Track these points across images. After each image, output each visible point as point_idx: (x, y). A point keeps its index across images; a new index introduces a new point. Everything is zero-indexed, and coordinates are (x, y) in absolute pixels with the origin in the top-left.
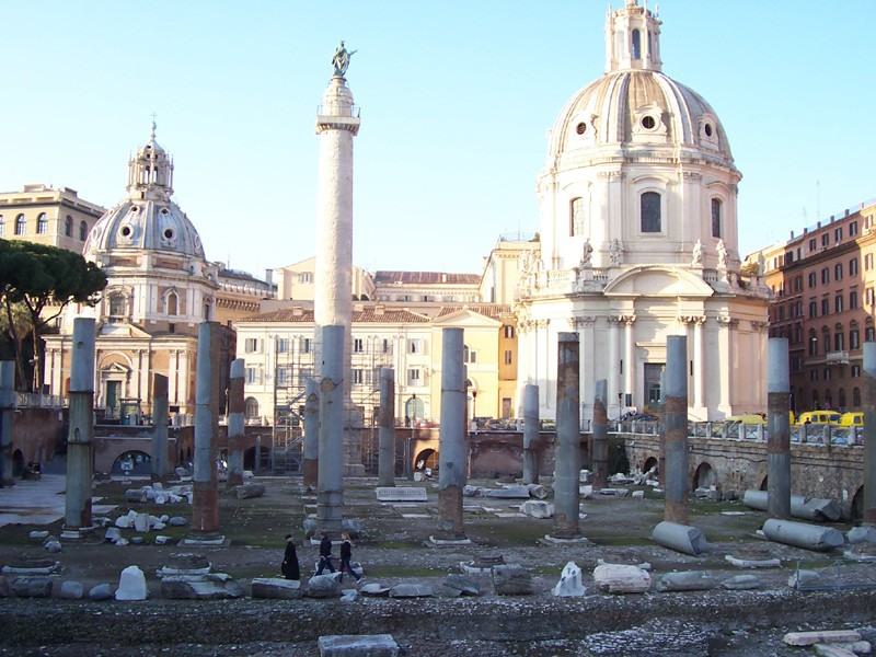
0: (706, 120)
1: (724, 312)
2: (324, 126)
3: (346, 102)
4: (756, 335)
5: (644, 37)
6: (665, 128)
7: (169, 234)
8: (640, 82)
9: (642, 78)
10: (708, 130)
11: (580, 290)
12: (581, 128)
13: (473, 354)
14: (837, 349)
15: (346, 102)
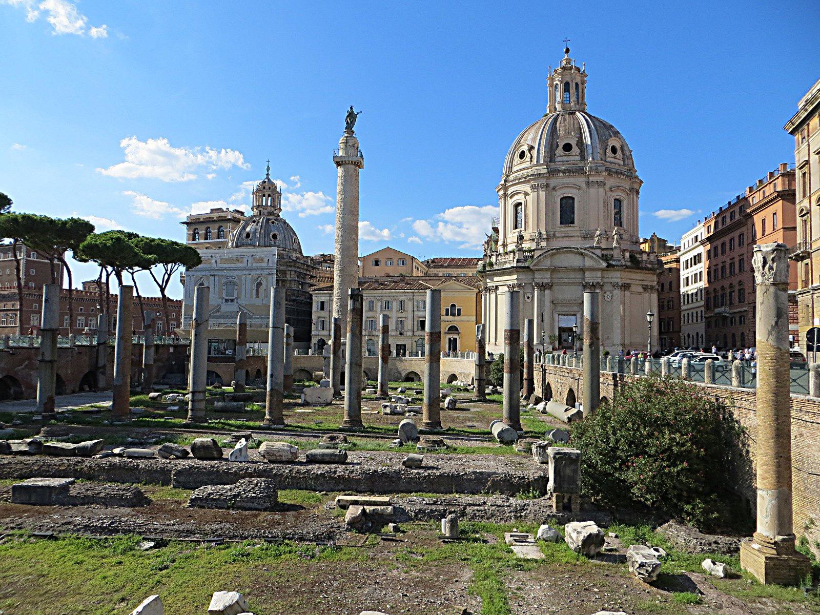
0: (613, 142)
1: (617, 276)
2: (338, 164)
3: (351, 144)
4: (647, 295)
5: (573, 86)
6: (579, 151)
7: (275, 237)
10: (614, 150)
11: (515, 265)
12: (522, 155)
13: (459, 310)
14: (722, 305)
15: (351, 144)
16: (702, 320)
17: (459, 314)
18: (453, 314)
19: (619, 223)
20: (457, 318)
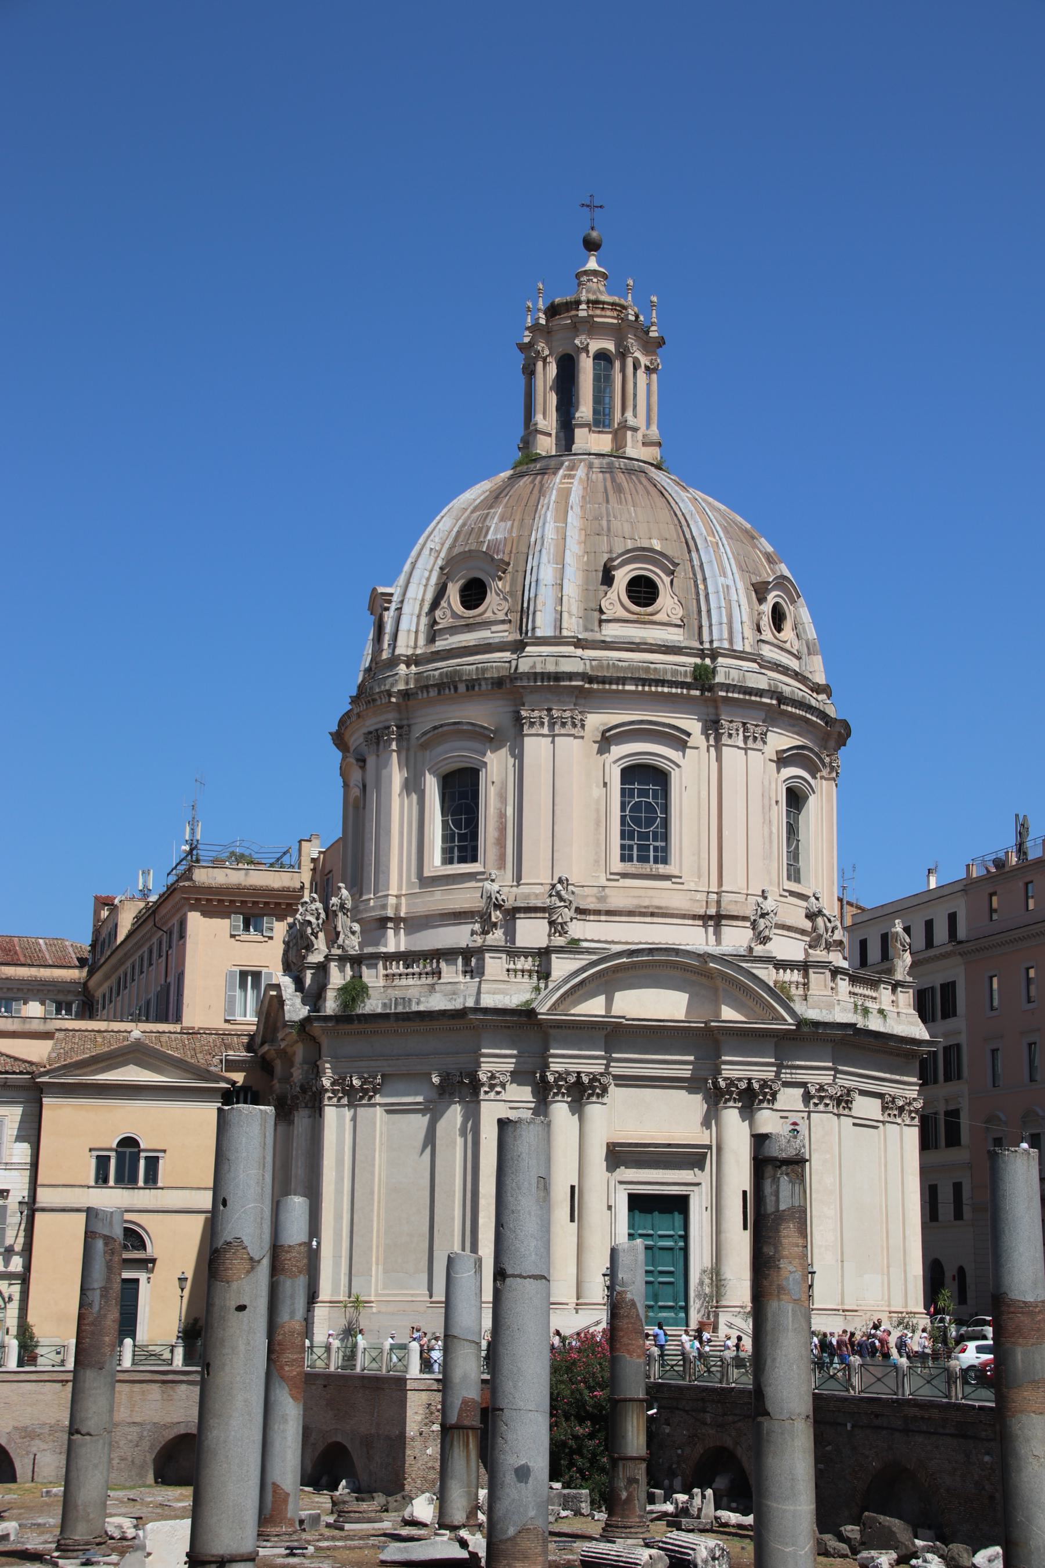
8: (619, 489)
9: (621, 478)
13: (153, 1163)
16: (958, 1215)
17: (152, 1178)
18: (127, 1178)
19: (794, 873)
20: (142, 1198)
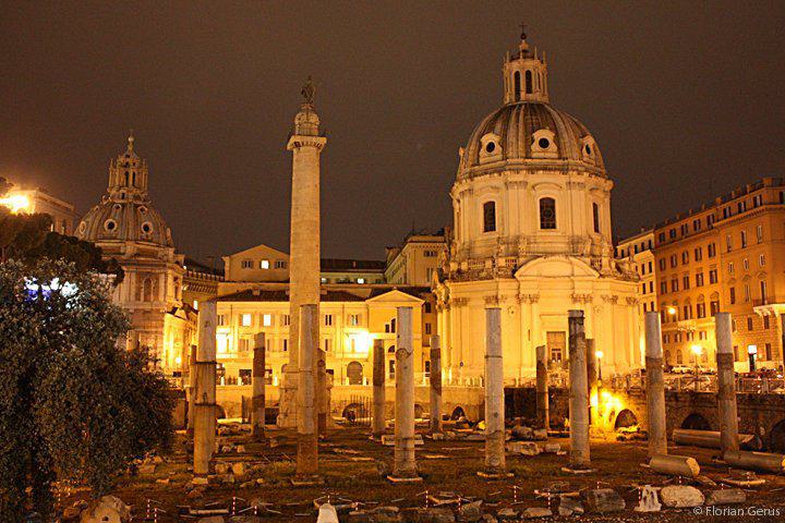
4: (630, 308)
